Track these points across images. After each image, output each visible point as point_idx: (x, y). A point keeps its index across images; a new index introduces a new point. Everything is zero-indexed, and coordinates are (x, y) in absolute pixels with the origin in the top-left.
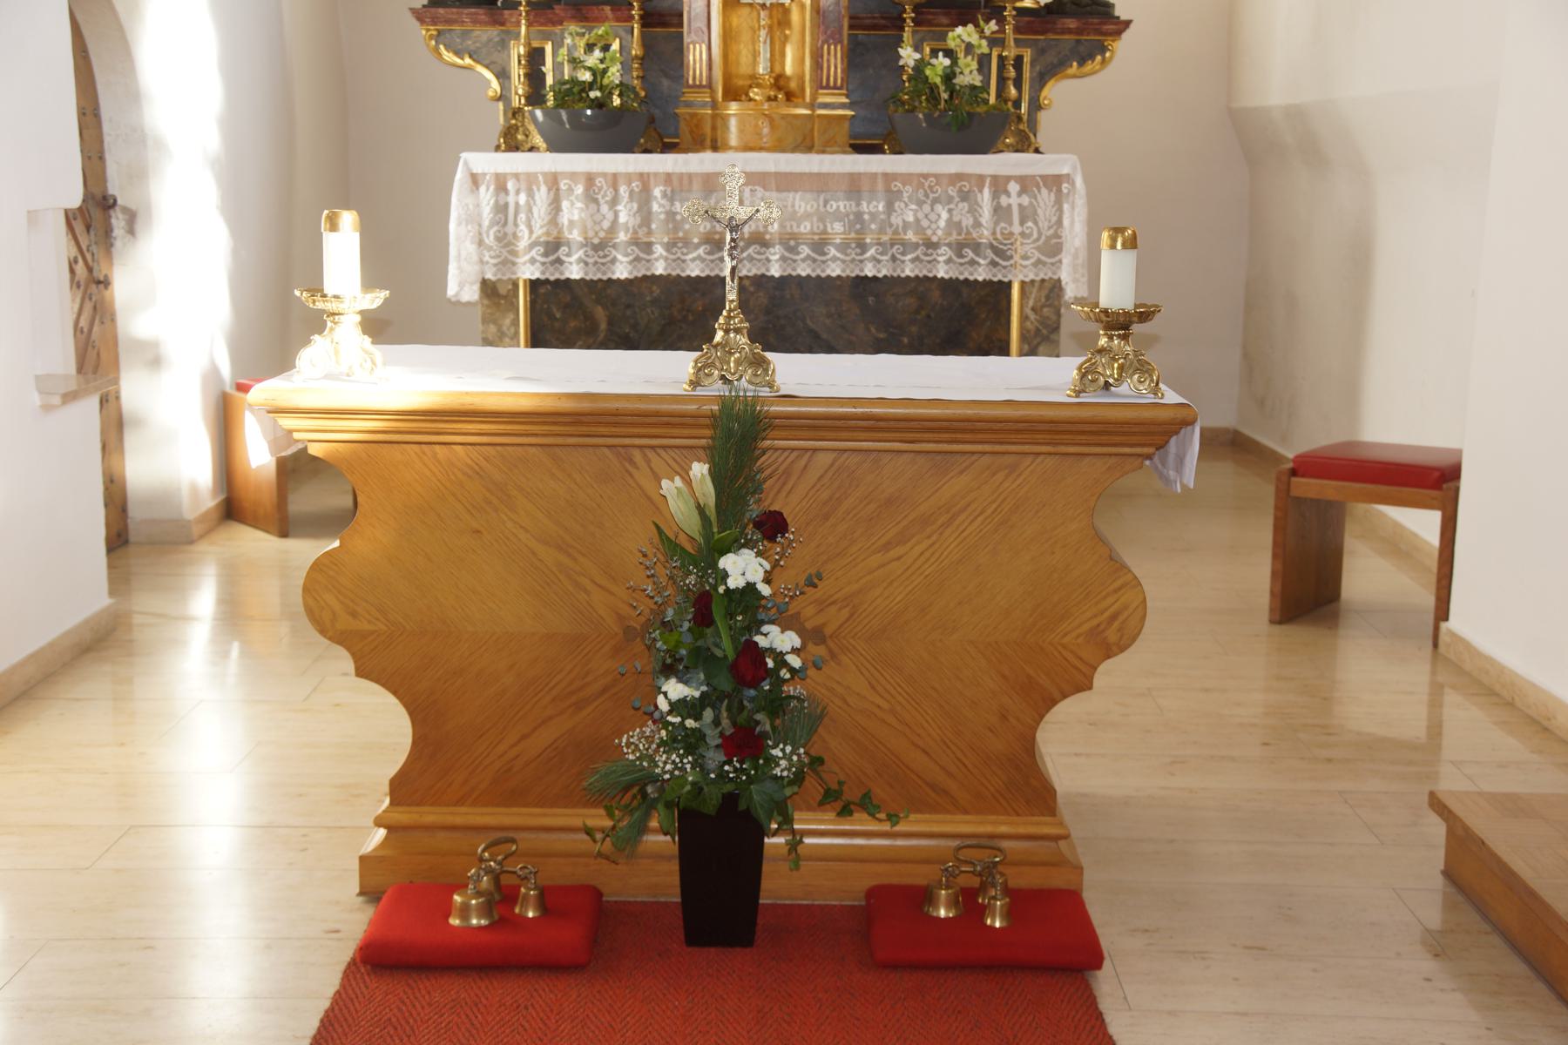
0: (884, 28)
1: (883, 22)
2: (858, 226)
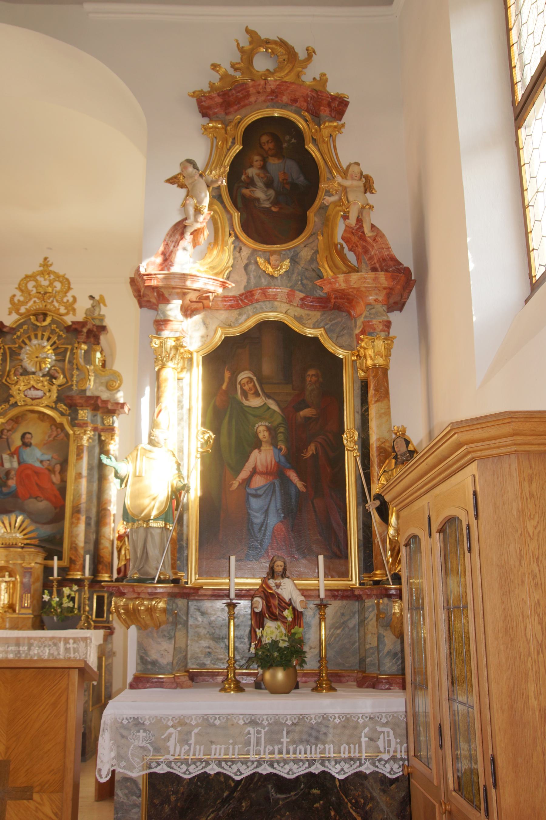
2: (19, 655)
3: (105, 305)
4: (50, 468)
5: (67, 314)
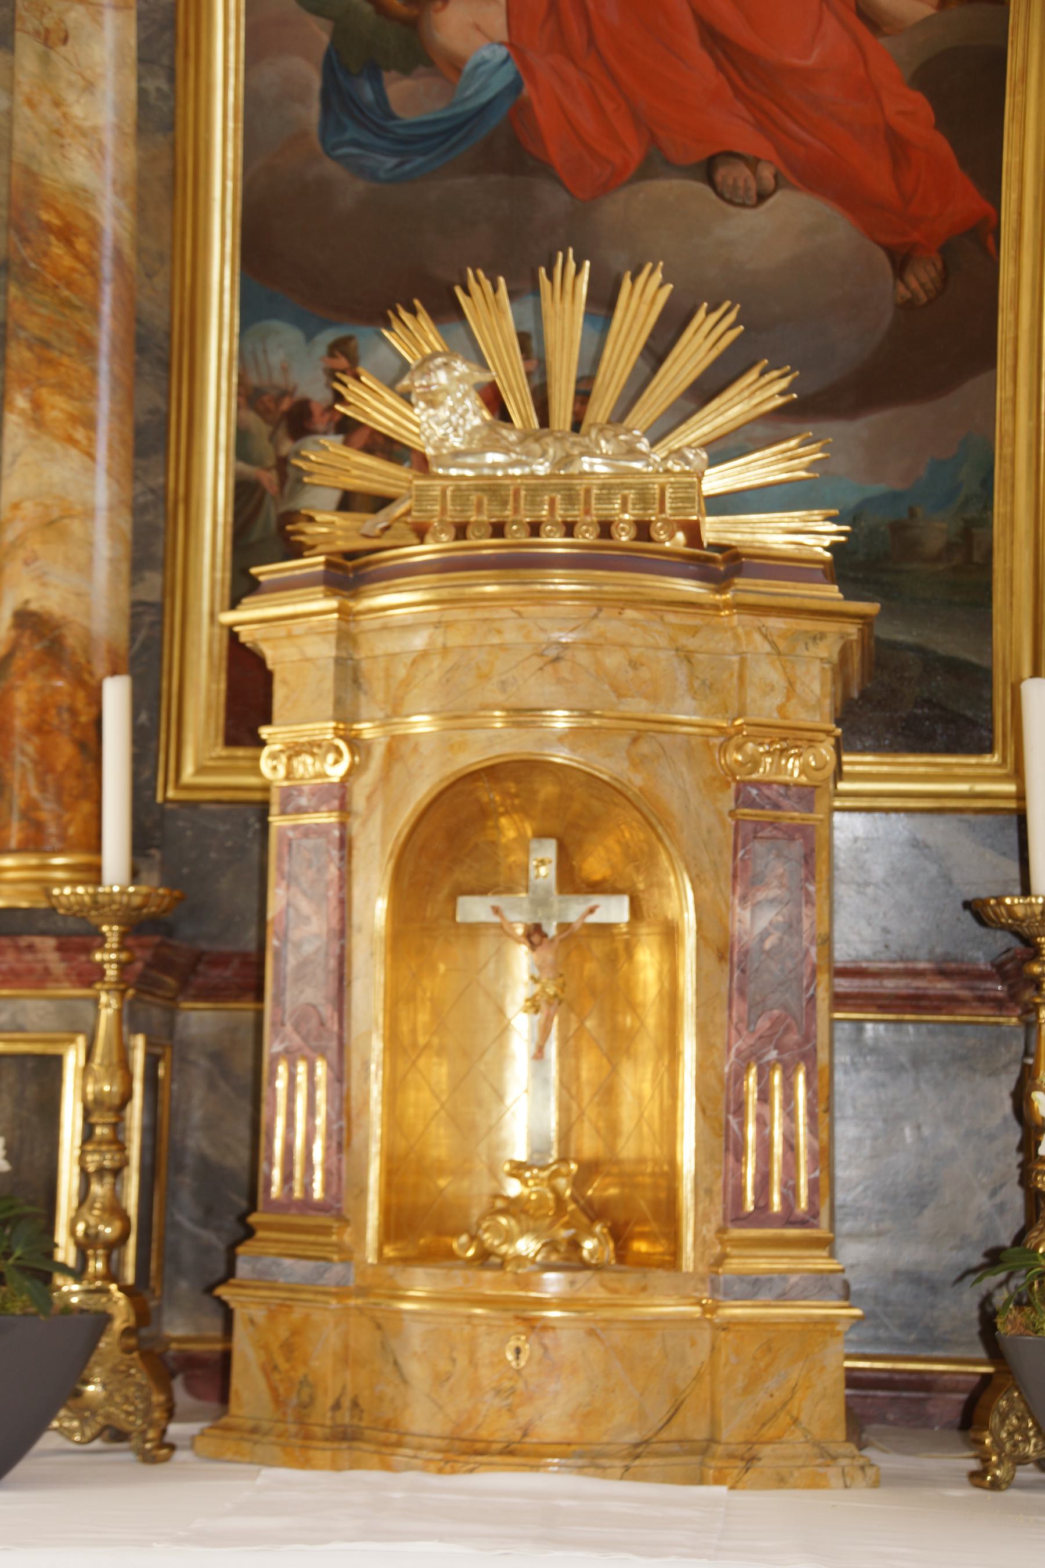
0: (947, 1003)
1: (943, 986)
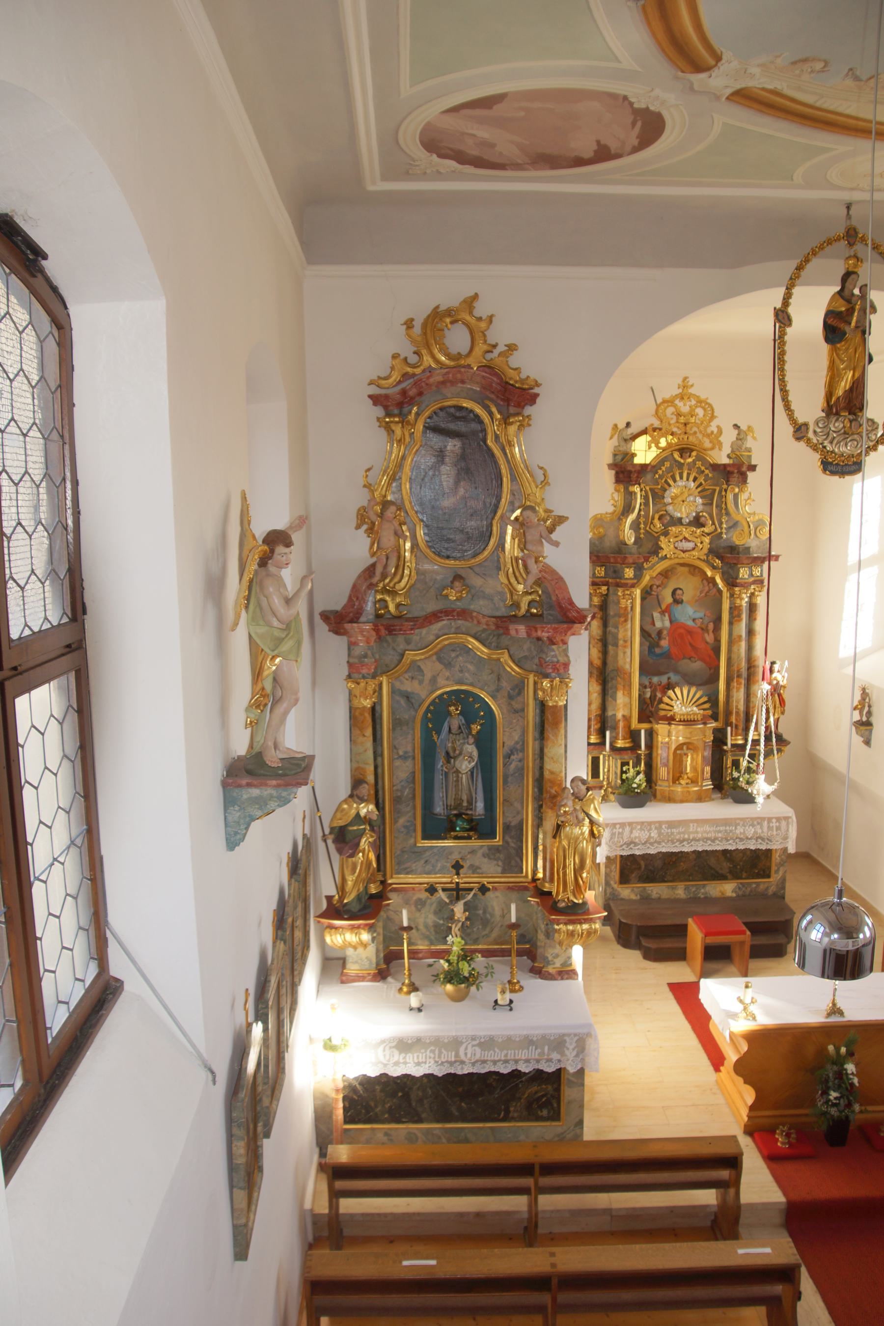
3: (754, 438)
4: (703, 626)
5: (712, 449)
